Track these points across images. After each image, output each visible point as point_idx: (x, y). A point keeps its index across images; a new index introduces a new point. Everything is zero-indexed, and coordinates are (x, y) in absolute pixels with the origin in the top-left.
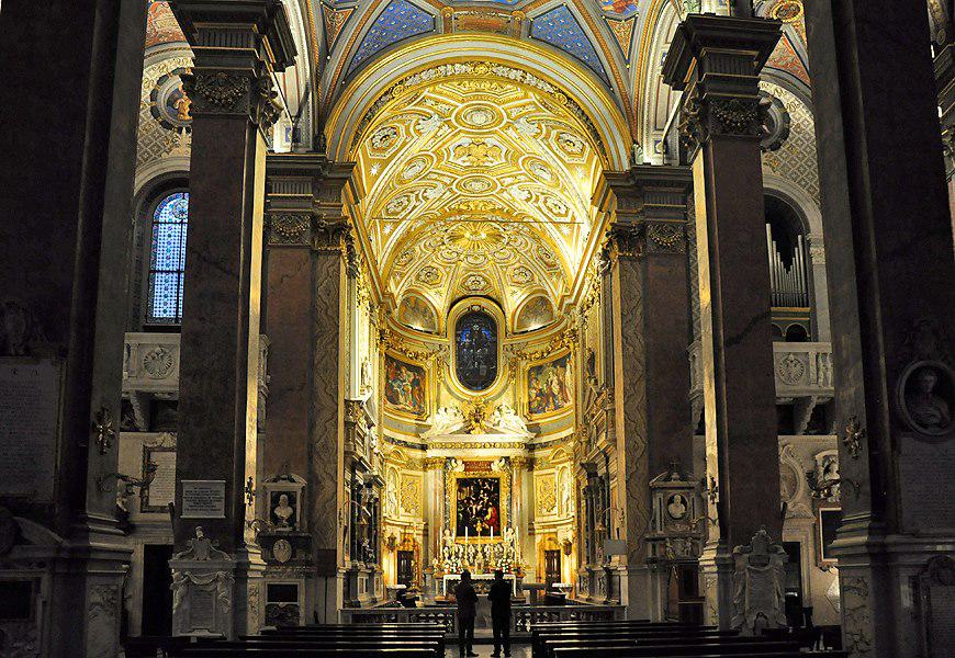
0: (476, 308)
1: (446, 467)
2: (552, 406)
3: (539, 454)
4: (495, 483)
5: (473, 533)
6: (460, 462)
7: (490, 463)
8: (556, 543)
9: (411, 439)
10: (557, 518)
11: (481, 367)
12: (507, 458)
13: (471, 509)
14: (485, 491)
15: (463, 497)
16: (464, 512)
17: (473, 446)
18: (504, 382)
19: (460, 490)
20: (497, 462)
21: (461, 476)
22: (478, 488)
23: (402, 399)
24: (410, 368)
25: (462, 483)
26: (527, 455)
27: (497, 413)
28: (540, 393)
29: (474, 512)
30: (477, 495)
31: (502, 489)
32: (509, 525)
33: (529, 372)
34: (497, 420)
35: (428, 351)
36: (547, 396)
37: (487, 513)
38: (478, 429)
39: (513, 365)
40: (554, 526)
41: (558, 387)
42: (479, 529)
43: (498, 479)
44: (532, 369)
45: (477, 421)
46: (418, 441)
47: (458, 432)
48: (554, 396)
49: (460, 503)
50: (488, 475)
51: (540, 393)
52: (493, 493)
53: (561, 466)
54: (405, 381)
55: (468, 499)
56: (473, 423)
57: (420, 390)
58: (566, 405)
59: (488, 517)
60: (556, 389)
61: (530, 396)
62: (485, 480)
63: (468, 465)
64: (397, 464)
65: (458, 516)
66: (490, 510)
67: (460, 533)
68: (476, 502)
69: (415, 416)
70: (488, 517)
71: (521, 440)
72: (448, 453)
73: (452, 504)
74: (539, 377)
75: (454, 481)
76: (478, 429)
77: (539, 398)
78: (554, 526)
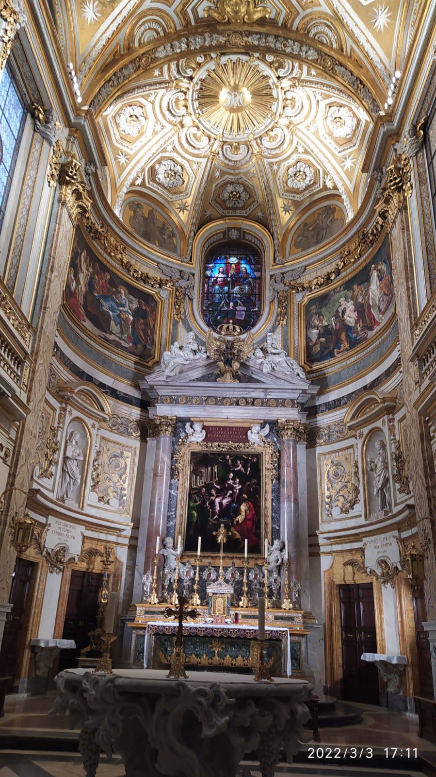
0: (234, 235)
1: (175, 433)
2: (345, 345)
3: (324, 420)
4: (254, 463)
5: (211, 546)
6: (197, 427)
7: (245, 431)
8: (362, 568)
9: (124, 387)
10: (362, 521)
11: (238, 308)
12: (273, 424)
13: (212, 503)
14: (237, 474)
15: (200, 483)
16: (201, 509)
17: (220, 401)
18: (270, 325)
19: (195, 472)
20: (256, 428)
21: (198, 449)
22: (226, 468)
23: (114, 327)
24: (133, 291)
25: (200, 460)
26: (304, 421)
27: (260, 353)
28: (326, 332)
29: (218, 508)
30: (223, 480)
31: (264, 472)
32: (276, 534)
33: (308, 307)
34: (259, 361)
35: (164, 278)
36: (338, 333)
37: (238, 512)
38: (228, 376)
39: (284, 301)
40: (357, 538)
41: (354, 315)
42: (221, 539)
43: (259, 456)
44: (312, 301)
45: (228, 362)
46: (135, 394)
47: (198, 380)
48: (348, 329)
49: (193, 493)
50: (242, 448)
51: (326, 332)
52: (249, 478)
53: (366, 430)
54: (124, 306)
55: (208, 487)
56: (221, 364)
57: (146, 324)
58: (371, 334)
59: (240, 518)
60: (351, 317)
61: (308, 339)
62: (237, 457)
63: (212, 433)
64: (90, 415)
65: (190, 515)
66: (243, 507)
67: (189, 546)
68: (221, 493)
69: (136, 359)
70: (240, 518)
71: (295, 396)
72: (180, 411)
73: (182, 496)
74: (323, 310)
75: (188, 457)
76: (228, 376)
77: (323, 340)
78: (357, 538)
